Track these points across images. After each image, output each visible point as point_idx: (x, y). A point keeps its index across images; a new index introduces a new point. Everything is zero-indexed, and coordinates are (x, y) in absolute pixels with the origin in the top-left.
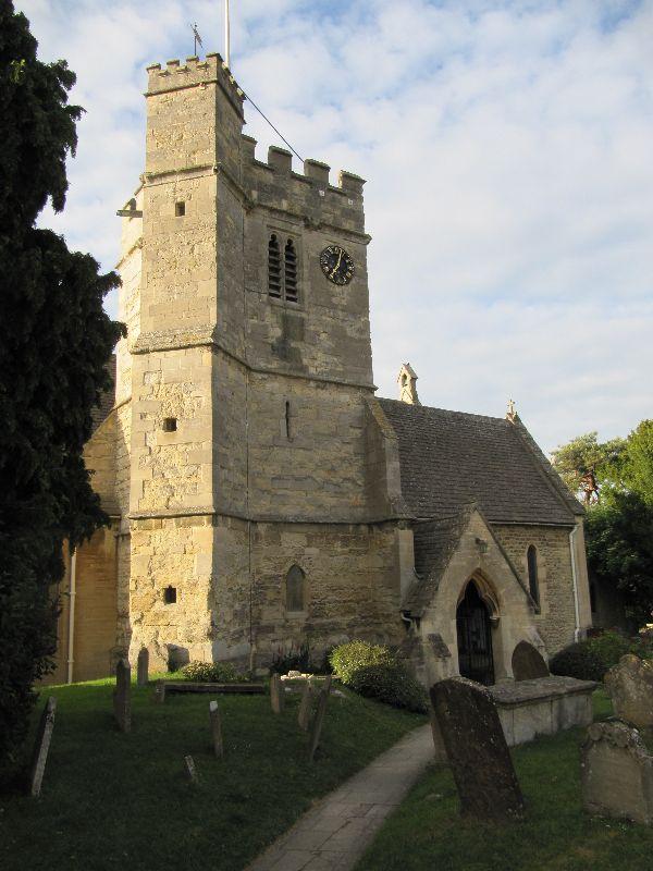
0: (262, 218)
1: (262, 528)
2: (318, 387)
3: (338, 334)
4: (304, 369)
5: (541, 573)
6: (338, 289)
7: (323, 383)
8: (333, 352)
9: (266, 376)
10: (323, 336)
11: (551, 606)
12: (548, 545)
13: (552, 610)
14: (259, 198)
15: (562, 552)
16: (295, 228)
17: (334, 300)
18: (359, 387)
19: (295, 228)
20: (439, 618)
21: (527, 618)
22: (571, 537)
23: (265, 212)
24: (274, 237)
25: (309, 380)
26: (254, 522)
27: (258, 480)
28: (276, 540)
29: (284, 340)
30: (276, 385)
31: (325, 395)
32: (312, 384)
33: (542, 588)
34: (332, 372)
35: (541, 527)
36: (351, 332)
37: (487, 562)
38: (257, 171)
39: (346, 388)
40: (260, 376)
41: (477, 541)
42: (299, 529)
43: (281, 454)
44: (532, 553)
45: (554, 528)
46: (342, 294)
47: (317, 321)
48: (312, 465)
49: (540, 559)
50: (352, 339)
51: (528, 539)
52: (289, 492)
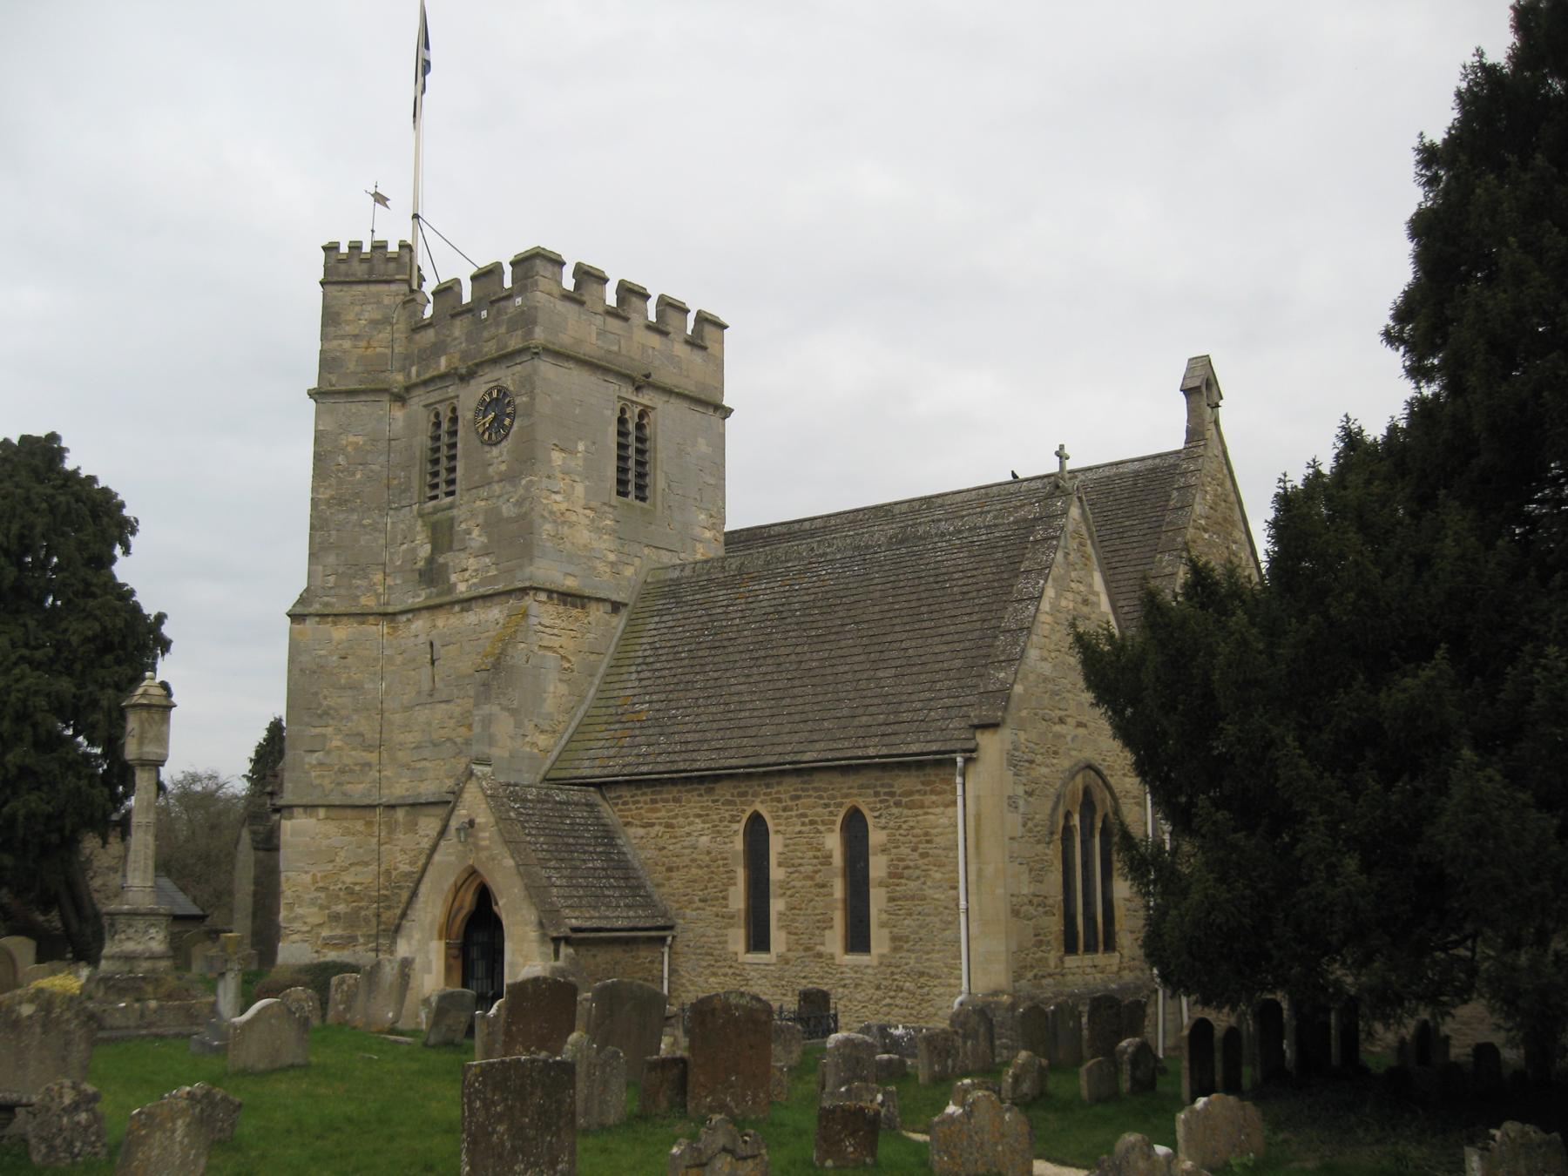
0: (418, 401)
1: (400, 814)
2: (462, 610)
3: (493, 522)
4: (452, 588)
5: (878, 867)
6: (495, 451)
7: (467, 603)
8: (485, 551)
9: (410, 616)
10: (476, 532)
11: (894, 939)
12: (897, 804)
13: (895, 949)
14: (418, 375)
15: (937, 818)
16: (451, 391)
17: (491, 470)
18: (509, 593)
19: (451, 391)
20: (417, 936)
21: (535, 945)
22: (959, 780)
23: (421, 391)
24: (437, 415)
25: (453, 603)
26: (392, 807)
27: (400, 754)
28: (412, 827)
29: (430, 561)
30: (420, 623)
31: (471, 618)
32: (457, 608)
33: (878, 899)
34: (484, 582)
35: (884, 767)
36: (508, 510)
37: (484, 855)
38: (417, 337)
39: (496, 600)
40: (404, 618)
41: (472, 823)
42: (431, 810)
43: (422, 715)
44: (855, 829)
45: (920, 765)
46: (500, 457)
47: (469, 511)
48: (452, 723)
49: (876, 837)
50: (510, 520)
51: (846, 796)
52: (426, 764)
